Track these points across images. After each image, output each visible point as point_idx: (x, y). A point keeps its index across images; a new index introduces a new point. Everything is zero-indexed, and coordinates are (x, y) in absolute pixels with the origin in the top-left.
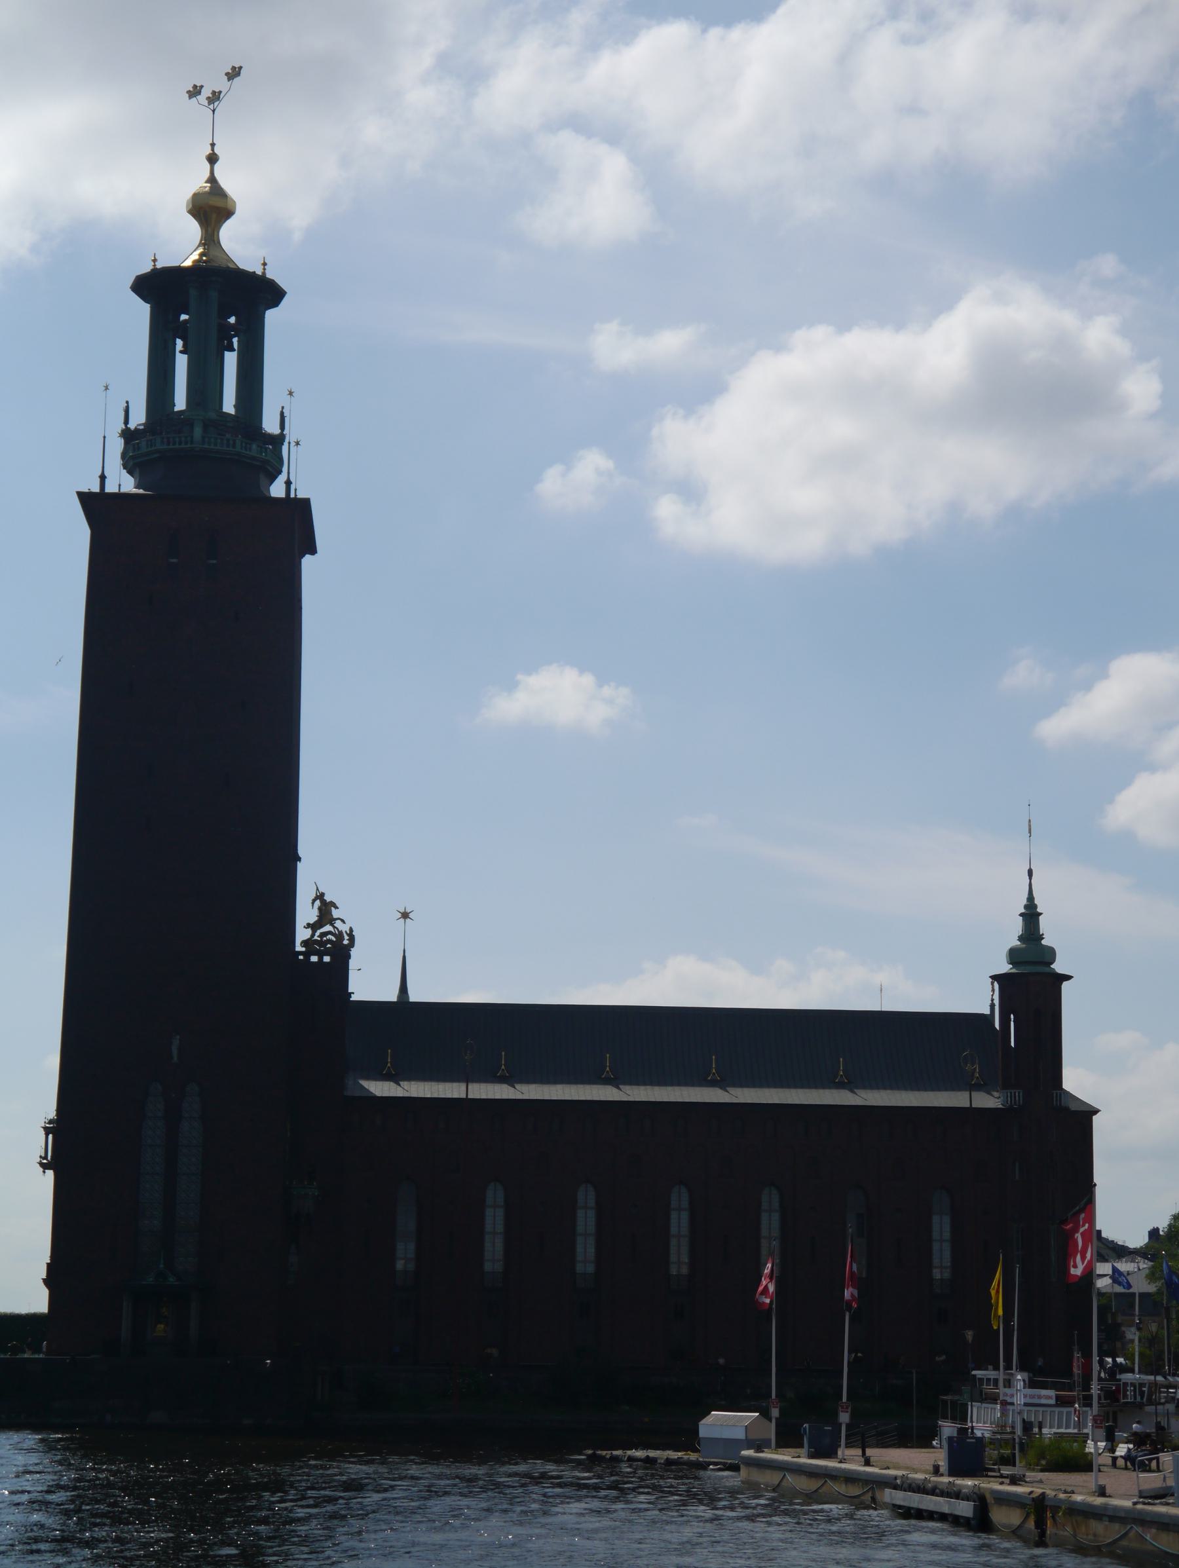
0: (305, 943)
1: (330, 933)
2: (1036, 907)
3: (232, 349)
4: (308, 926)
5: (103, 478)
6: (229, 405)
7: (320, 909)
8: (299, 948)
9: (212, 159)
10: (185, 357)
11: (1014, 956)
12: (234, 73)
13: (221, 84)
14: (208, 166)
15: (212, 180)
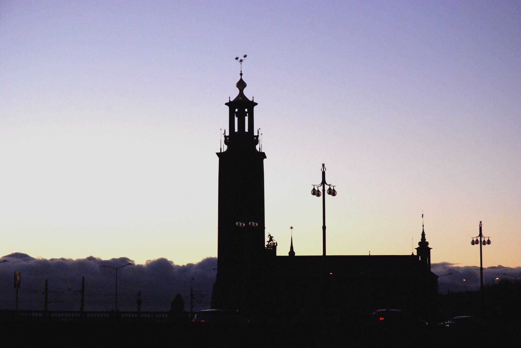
0: (267, 245)
1: (272, 243)
2: (424, 233)
3: (247, 116)
4: (267, 242)
5: (221, 149)
6: (247, 130)
7: (270, 238)
8: (266, 247)
9: (241, 74)
10: (237, 118)
11: (420, 243)
12: (245, 56)
13: (243, 58)
14: (240, 76)
15: (241, 80)
